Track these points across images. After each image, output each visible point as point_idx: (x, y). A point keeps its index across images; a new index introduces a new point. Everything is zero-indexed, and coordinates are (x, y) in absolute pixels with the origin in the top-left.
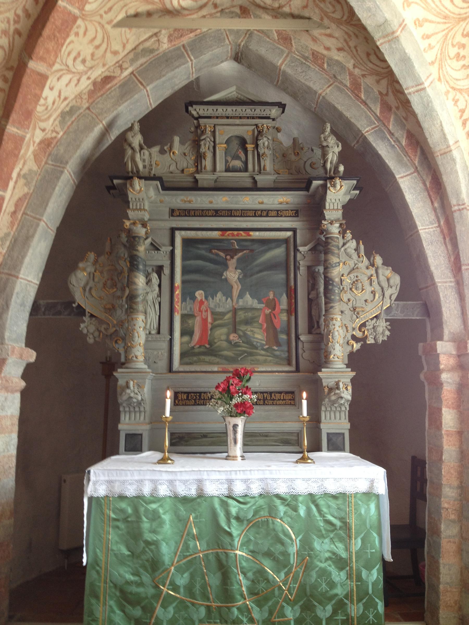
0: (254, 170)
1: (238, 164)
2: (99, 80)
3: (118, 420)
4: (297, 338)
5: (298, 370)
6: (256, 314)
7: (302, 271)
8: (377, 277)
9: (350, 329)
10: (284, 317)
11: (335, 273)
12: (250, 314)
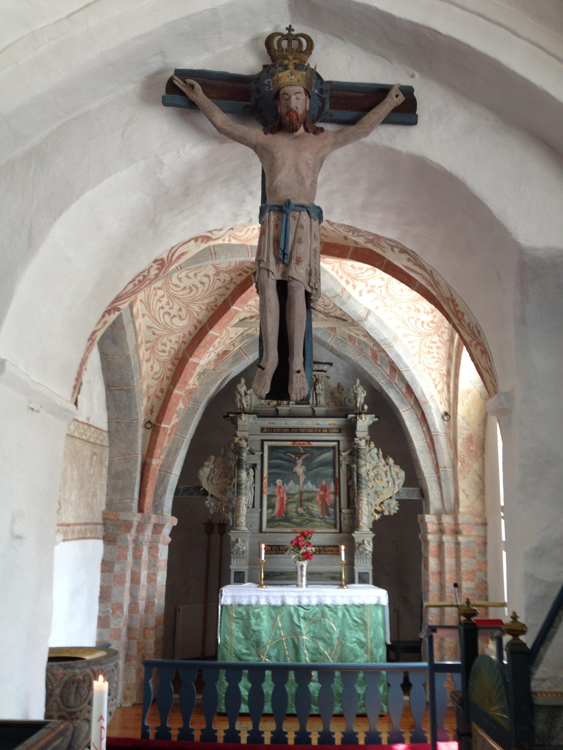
0: (313, 404)
2: (221, 353)
3: (230, 563)
4: (340, 511)
5: (341, 532)
6: (315, 494)
7: (344, 468)
8: (391, 472)
9: (373, 505)
10: (332, 497)
11: (363, 471)
12: (310, 495)
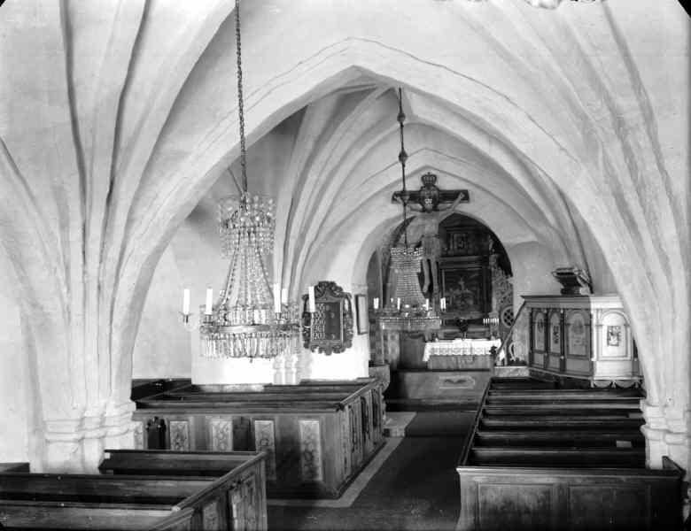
1: (461, 246)
